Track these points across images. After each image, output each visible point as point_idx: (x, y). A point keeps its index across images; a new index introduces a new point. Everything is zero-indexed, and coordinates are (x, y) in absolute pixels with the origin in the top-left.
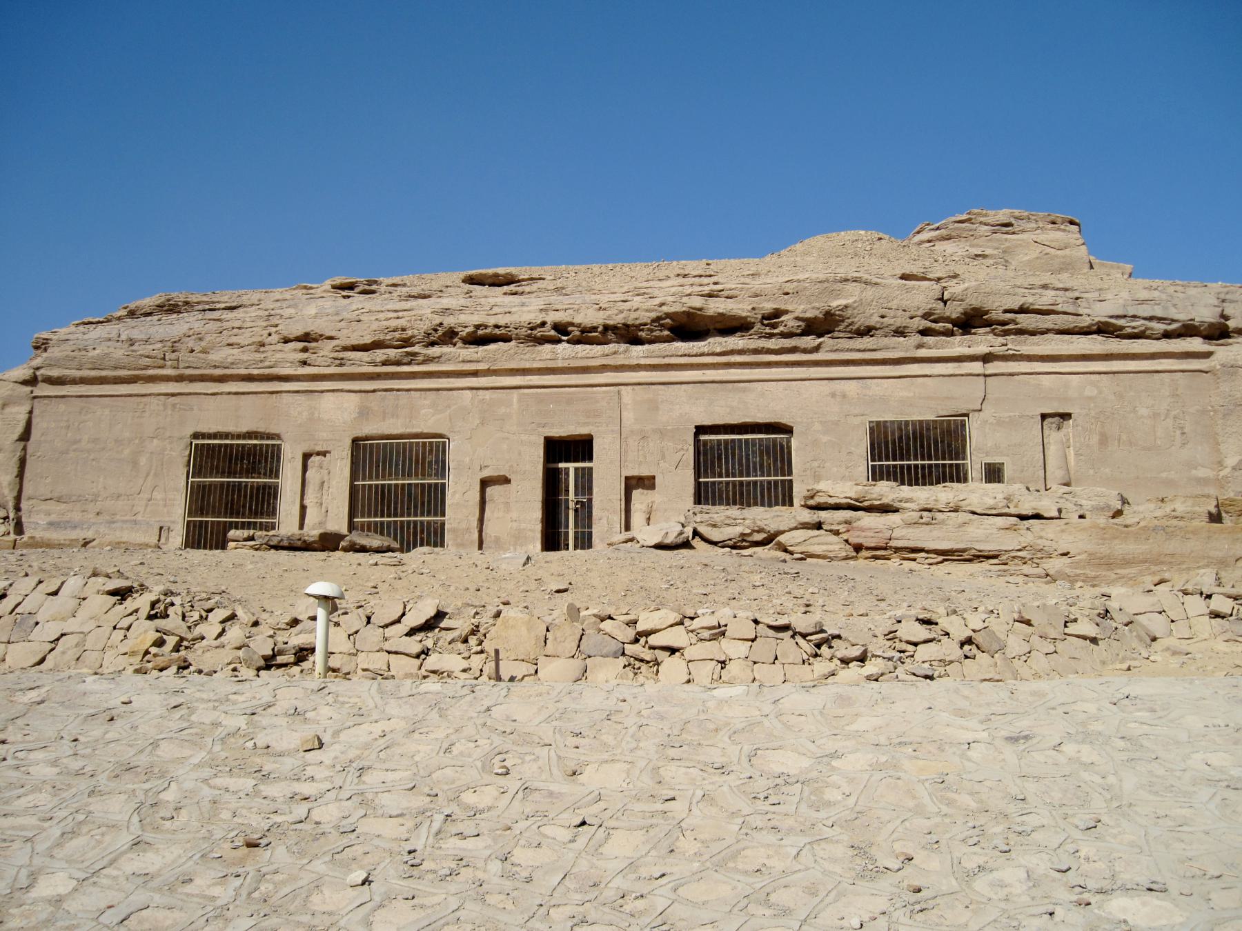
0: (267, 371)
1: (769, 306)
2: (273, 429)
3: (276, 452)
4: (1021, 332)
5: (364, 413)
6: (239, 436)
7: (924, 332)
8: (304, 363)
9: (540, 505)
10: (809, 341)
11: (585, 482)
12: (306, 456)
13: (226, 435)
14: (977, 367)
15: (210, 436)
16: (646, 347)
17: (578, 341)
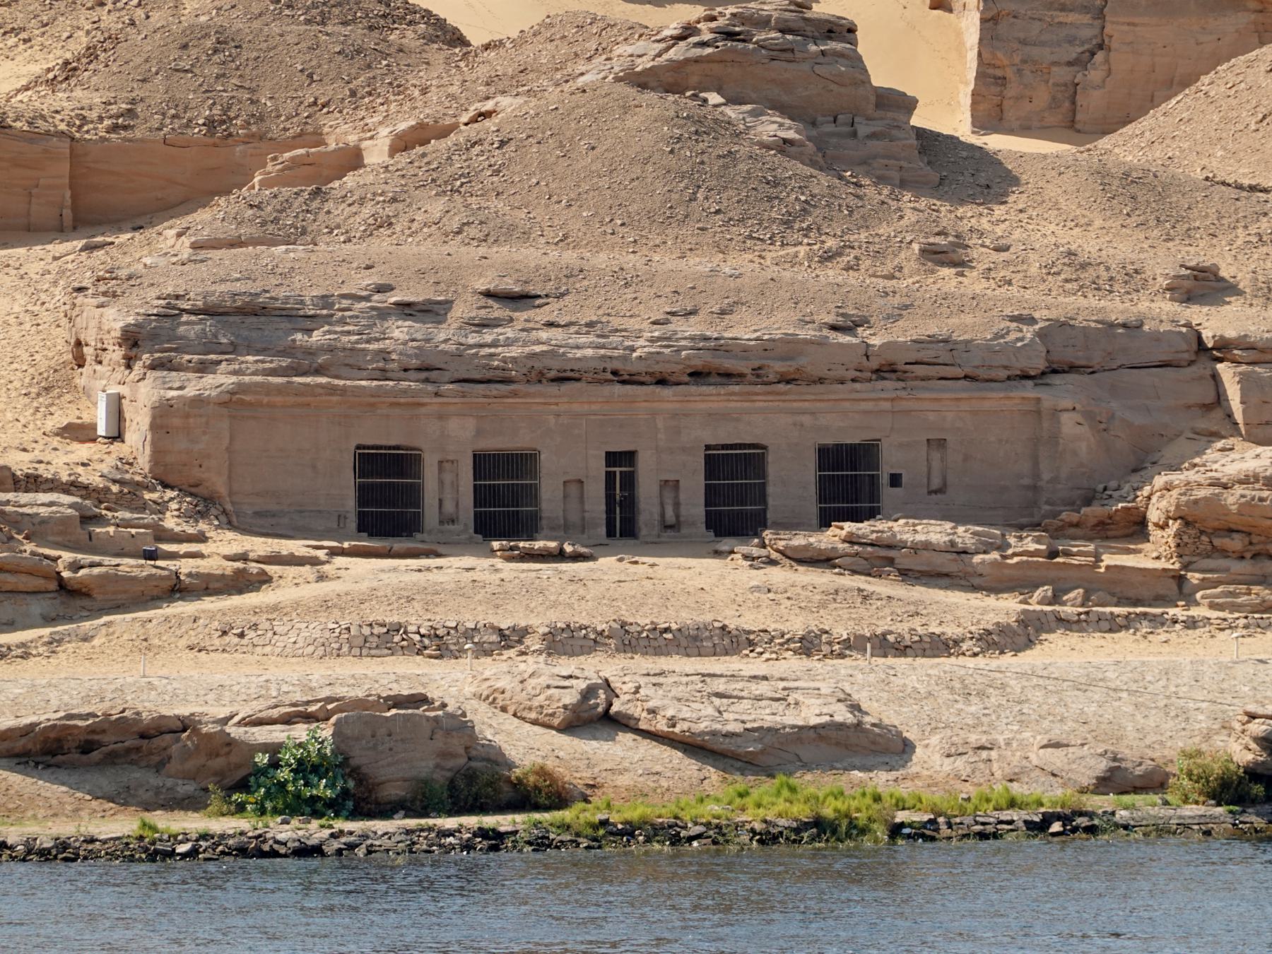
0: (410, 400)
1: (757, 364)
2: (415, 444)
3: (418, 459)
4: (916, 378)
5: (479, 433)
6: (390, 448)
7: (853, 380)
8: (436, 394)
9: (604, 500)
10: (781, 387)
11: (629, 481)
12: (440, 462)
13: (380, 447)
14: (886, 405)
15: (369, 448)
16: (674, 387)
17: (624, 382)
